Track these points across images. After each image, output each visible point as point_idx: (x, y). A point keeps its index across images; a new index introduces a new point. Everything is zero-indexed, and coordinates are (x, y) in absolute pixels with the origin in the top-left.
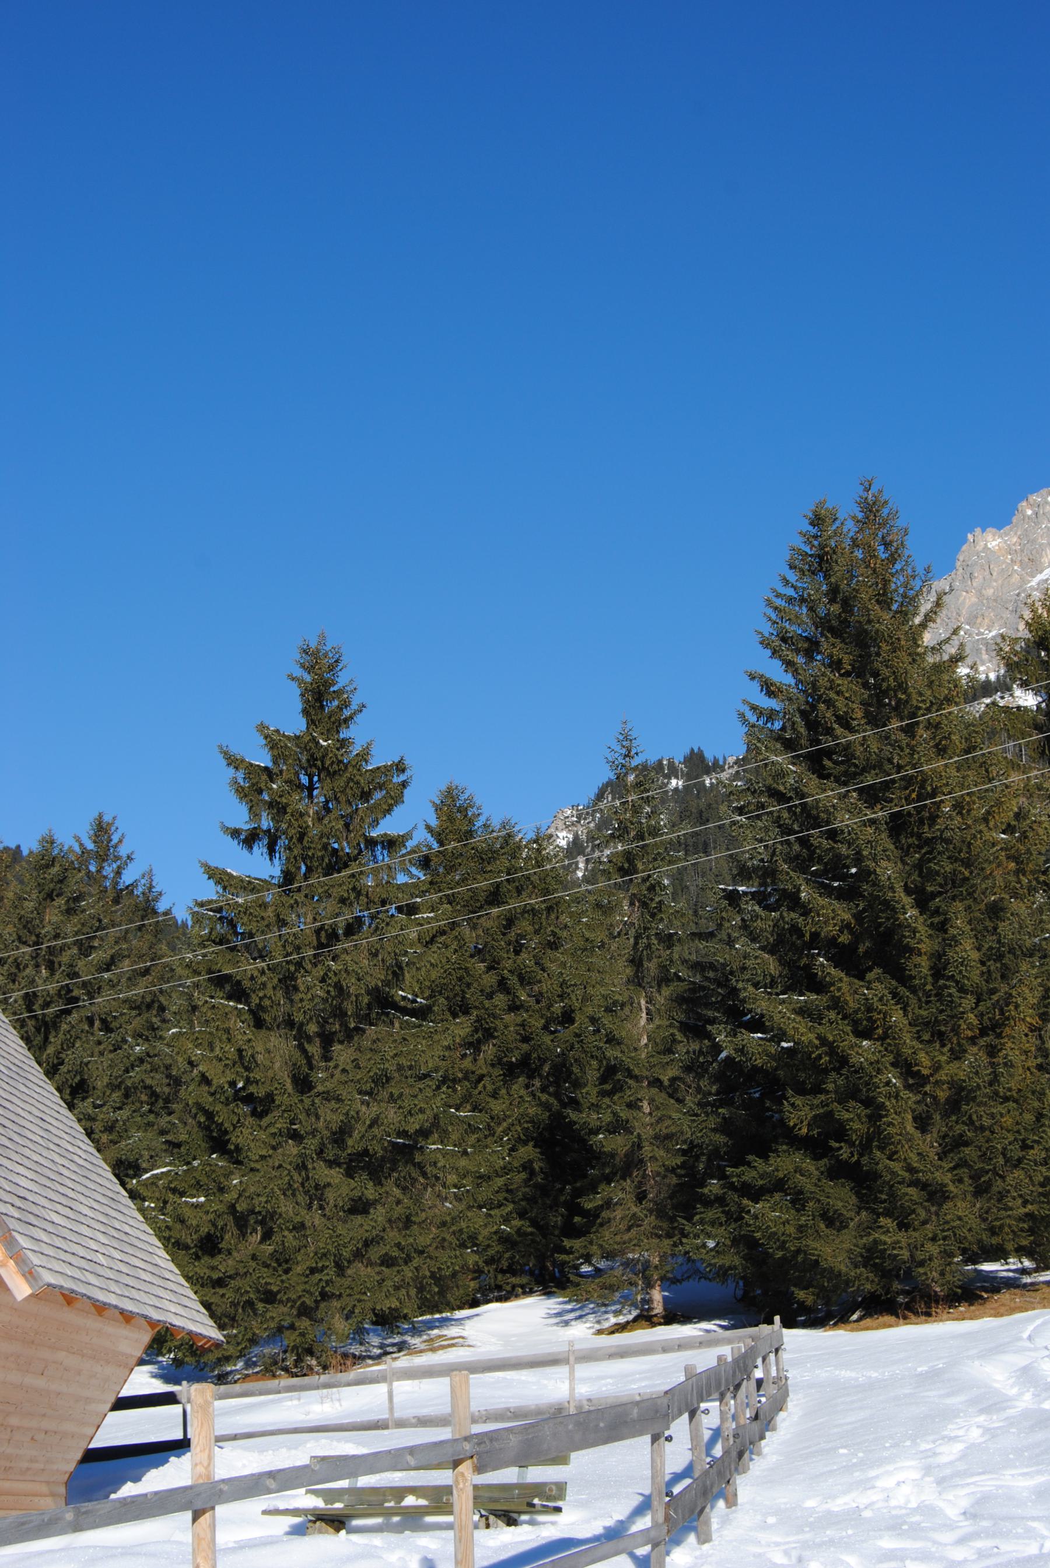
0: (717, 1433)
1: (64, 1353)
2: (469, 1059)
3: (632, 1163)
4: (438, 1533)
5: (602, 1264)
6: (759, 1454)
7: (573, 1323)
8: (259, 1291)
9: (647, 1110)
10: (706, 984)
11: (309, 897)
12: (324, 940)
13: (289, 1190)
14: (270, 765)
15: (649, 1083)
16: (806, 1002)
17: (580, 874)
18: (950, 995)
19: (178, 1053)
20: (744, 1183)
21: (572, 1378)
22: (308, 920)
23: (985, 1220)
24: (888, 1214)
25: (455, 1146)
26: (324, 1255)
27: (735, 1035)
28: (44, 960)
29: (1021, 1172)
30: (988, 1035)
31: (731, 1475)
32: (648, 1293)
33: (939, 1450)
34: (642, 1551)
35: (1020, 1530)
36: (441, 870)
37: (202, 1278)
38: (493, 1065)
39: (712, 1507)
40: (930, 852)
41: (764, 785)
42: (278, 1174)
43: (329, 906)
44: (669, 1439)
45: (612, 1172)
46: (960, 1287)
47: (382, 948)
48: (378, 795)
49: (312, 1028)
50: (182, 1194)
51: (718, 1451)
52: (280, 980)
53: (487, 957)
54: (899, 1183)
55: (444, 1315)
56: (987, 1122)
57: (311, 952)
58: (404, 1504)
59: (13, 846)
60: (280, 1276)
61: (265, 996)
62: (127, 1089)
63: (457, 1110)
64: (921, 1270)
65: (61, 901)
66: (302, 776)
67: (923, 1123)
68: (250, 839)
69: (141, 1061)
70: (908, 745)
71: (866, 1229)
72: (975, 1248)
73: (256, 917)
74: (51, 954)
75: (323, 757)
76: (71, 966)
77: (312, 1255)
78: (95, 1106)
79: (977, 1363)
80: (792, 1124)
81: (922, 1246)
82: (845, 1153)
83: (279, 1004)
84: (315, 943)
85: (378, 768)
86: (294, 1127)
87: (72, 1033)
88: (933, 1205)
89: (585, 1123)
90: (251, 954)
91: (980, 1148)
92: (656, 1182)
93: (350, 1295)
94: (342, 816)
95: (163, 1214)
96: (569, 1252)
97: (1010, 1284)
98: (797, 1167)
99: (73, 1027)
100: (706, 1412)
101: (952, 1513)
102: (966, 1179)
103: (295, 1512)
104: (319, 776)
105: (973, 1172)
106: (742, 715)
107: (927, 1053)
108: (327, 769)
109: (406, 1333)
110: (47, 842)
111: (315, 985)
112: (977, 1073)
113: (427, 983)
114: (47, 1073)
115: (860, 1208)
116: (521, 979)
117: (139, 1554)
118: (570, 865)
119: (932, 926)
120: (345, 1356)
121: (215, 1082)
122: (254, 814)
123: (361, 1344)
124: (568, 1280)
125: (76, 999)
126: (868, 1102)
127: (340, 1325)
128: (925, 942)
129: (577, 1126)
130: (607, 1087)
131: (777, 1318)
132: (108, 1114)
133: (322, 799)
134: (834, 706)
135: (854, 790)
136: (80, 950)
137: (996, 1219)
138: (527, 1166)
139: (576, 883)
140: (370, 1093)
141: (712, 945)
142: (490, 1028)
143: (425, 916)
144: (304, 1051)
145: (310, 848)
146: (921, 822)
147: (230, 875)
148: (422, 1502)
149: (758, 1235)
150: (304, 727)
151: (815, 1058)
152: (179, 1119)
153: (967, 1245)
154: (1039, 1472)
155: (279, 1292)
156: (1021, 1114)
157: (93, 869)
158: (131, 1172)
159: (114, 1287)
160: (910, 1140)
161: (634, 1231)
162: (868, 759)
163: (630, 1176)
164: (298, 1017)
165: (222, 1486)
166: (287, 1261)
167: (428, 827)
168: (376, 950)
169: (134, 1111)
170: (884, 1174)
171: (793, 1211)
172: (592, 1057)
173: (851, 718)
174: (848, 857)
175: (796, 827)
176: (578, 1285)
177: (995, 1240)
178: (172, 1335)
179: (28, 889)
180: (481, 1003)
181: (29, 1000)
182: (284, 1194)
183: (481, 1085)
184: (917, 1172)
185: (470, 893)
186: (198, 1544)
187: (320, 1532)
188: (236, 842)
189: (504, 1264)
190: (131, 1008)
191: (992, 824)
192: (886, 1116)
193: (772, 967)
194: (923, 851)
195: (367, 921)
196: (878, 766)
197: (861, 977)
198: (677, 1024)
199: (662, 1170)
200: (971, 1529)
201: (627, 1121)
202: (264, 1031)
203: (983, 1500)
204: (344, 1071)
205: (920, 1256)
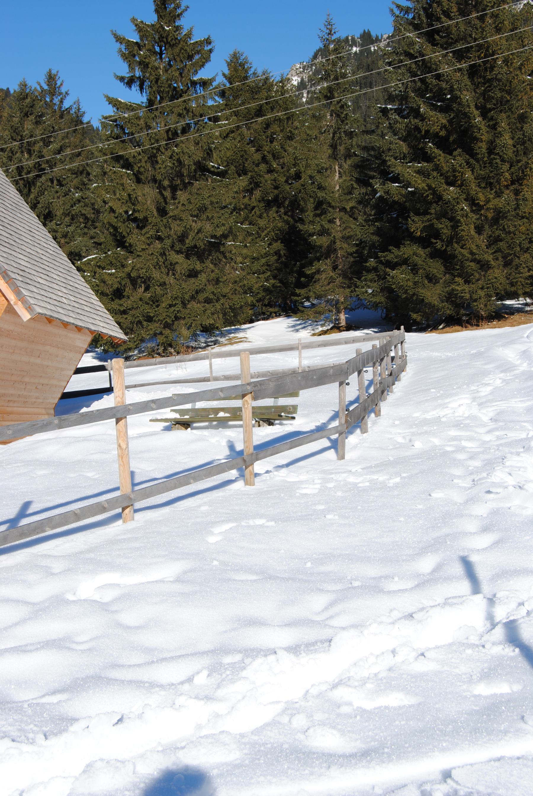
0: (371, 382)
1: (49, 347)
2: (247, 198)
3: (330, 251)
4: (235, 429)
5: (315, 302)
6: (392, 392)
7: (301, 330)
8: (144, 316)
9: (339, 224)
10: (369, 158)
11: (162, 113)
12: (170, 136)
13: (157, 266)
14: (139, 41)
15: (340, 211)
16: (421, 167)
17: (304, 100)
18: (497, 163)
19: (98, 197)
20: (387, 261)
21: (300, 357)
22: (162, 126)
23: (508, 279)
24: (459, 276)
25: (241, 243)
26: (176, 298)
27: (384, 185)
28: (26, 149)
29: (528, 255)
30: (515, 184)
31: (378, 402)
32: (338, 316)
33: (480, 390)
34: (334, 437)
35: (518, 427)
36: (231, 98)
37: (116, 310)
38: (259, 201)
39: (368, 417)
40: (489, 87)
41: (403, 50)
42: (151, 258)
43: (173, 118)
44: (348, 384)
45: (320, 255)
46: (494, 312)
47: (201, 140)
48: (197, 57)
49: (166, 183)
50: (103, 269)
51: (372, 390)
52: (148, 158)
53: (256, 144)
54: (466, 260)
55: (236, 327)
56: (512, 229)
57: (164, 143)
58: (218, 416)
59: (5, 88)
60: (154, 308)
61: (141, 166)
62: (73, 216)
63: (241, 224)
64: (475, 304)
65: (32, 117)
66: (156, 47)
67: (479, 230)
68: (130, 82)
69: (79, 201)
70: (481, 27)
71: (448, 283)
72: (503, 292)
73: (135, 124)
74: (29, 146)
75: (167, 36)
76: (40, 152)
77: (170, 298)
78: (57, 225)
79: (501, 349)
80: (412, 230)
81: (476, 292)
82: (439, 245)
83: (149, 170)
84: (166, 138)
85: (197, 42)
86: (158, 234)
87: (43, 187)
88: (482, 271)
89: (306, 230)
90: (133, 144)
91: (508, 242)
92: (342, 260)
93: (189, 318)
94: (178, 69)
95: (94, 279)
96: (299, 295)
97: (519, 311)
98: (414, 252)
99: (43, 184)
100: (367, 371)
101: (485, 419)
102: (500, 258)
103: (166, 420)
104: (165, 47)
105: (504, 255)
106: (392, 11)
107: (483, 194)
108: (169, 43)
109: (218, 336)
110: (23, 85)
111: (167, 160)
112: (508, 204)
113: (225, 159)
114: (31, 208)
115: (446, 273)
116: (274, 156)
117: (91, 440)
118: (299, 94)
119: (489, 126)
120: (188, 347)
121: (117, 211)
122: (132, 68)
123: (196, 341)
124: (298, 309)
125: (44, 169)
126: (452, 219)
127: (185, 332)
128: (485, 135)
129: (303, 232)
130: (318, 212)
131: (402, 327)
132: (63, 229)
133: (167, 60)
134: (442, 5)
135: (451, 52)
136: (44, 143)
137: (514, 278)
138: (277, 253)
139: (302, 105)
140: (197, 216)
141: (374, 137)
142: (258, 182)
143: (223, 122)
144: (162, 195)
145: (161, 87)
146: (486, 69)
147: (120, 102)
148: (227, 415)
149: (394, 286)
150: (156, 20)
151: (425, 197)
152: (100, 231)
153: (499, 291)
154: (528, 400)
155: (154, 316)
156: (530, 225)
157: (48, 100)
158: (77, 258)
159: (71, 314)
160: (472, 238)
161: (331, 285)
162: (459, 35)
163: (330, 257)
164: (158, 177)
165: (130, 407)
166: (157, 301)
167: (224, 75)
168: (198, 141)
169: (77, 227)
170: (458, 255)
171: (412, 275)
172: (310, 196)
173: (450, 12)
174: (446, 89)
175: (419, 73)
176: (303, 312)
177: (513, 289)
178: (102, 338)
179: (15, 111)
180: (253, 169)
181: (20, 170)
182: (155, 268)
183: (253, 212)
184: (475, 254)
185: (246, 110)
186: (119, 434)
187: (178, 429)
188: (122, 84)
189: (266, 302)
190: (72, 174)
191: (523, 71)
192: (461, 226)
193: (404, 148)
194: (486, 86)
195: (193, 126)
196: (464, 39)
197: (451, 154)
198: (354, 179)
199: (345, 254)
200: (494, 426)
201: (328, 230)
202: (141, 184)
203: (500, 413)
204: (183, 205)
205: (475, 296)
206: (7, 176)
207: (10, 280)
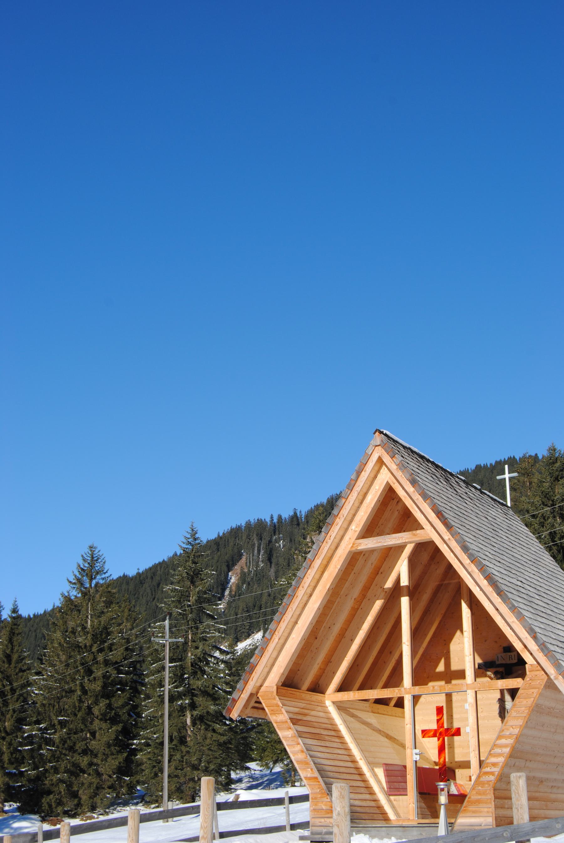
28: (558, 513)
59: (533, 454)
110: (552, 450)
179: (545, 476)
181: (552, 535)
206: (540, 542)
207: (549, 652)
